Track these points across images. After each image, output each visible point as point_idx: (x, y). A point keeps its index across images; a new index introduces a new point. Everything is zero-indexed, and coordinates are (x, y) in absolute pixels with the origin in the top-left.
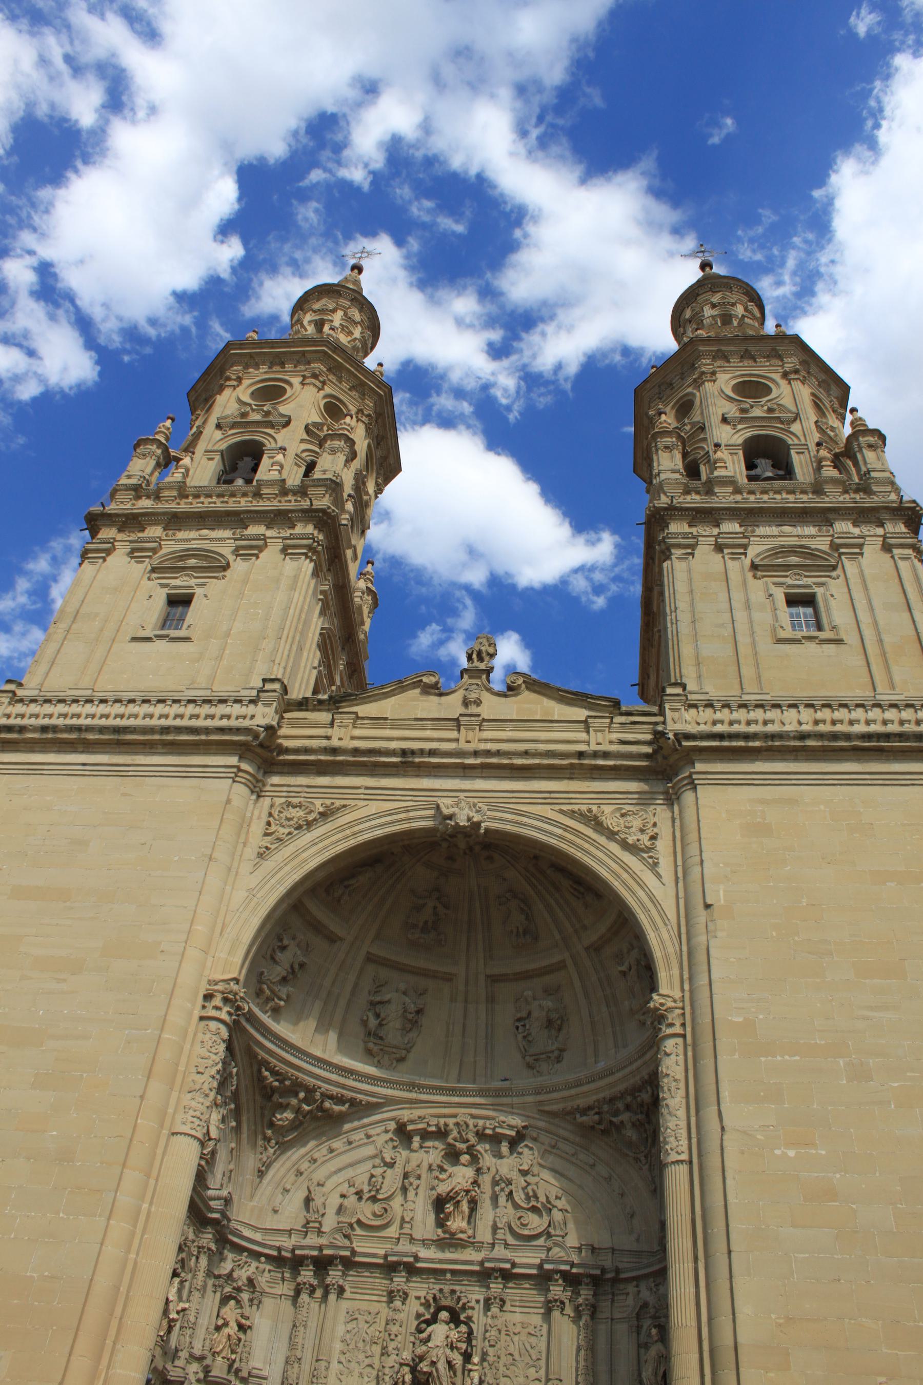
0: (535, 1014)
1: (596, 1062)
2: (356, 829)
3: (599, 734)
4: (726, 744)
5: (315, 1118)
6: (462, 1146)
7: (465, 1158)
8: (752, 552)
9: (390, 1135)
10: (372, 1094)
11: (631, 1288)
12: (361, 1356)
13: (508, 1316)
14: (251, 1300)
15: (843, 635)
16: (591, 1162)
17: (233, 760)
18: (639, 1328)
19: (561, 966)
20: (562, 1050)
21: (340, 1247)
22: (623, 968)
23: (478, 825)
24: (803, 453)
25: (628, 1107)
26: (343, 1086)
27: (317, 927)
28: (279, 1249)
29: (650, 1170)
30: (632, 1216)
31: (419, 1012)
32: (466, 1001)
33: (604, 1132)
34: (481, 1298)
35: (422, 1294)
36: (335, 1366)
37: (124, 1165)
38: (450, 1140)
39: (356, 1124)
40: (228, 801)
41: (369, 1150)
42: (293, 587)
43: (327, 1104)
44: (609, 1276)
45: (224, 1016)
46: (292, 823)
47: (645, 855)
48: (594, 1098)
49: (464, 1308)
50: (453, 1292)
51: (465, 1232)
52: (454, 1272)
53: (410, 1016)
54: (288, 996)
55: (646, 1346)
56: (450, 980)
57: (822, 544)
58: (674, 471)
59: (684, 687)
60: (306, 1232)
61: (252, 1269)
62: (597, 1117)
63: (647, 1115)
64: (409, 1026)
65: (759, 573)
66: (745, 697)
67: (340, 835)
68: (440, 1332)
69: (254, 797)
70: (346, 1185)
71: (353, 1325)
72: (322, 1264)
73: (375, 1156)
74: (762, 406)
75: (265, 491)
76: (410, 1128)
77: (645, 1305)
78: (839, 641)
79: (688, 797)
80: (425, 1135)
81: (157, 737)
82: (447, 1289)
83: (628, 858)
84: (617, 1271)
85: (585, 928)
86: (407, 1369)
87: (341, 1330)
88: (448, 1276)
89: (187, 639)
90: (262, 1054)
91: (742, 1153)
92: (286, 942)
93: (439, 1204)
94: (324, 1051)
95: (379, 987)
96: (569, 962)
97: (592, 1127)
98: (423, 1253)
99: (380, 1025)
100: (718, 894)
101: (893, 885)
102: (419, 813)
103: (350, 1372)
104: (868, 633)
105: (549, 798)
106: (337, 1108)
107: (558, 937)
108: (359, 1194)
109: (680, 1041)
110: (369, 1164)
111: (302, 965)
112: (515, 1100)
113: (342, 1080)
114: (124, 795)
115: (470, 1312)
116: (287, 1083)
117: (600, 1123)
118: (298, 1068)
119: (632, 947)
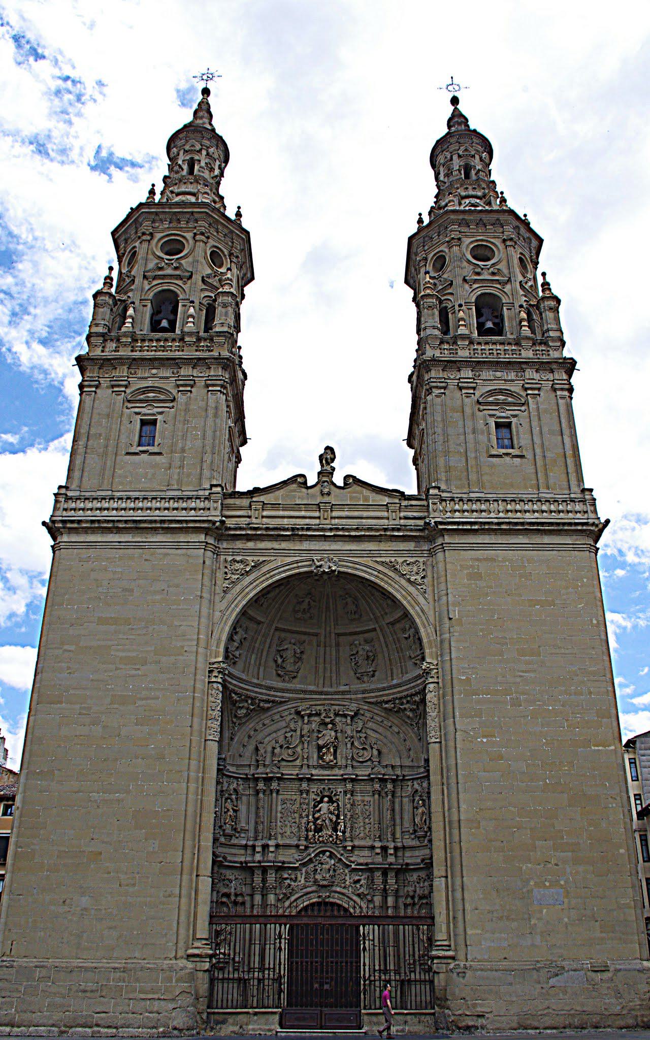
0: (361, 653)
1: (392, 680)
2: (272, 574)
3: (394, 514)
4: (460, 527)
5: (257, 711)
6: (328, 720)
7: (330, 726)
8: (478, 393)
9: (292, 716)
10: (283, 697)
11: (410, 783)
12: (290, 819)
13: (355, 798)
14: (237, 799)
15: (525, 453)
16: (390, 725)
17: (202, 537)
18: (414, 800)
19: (374, 630)
20: (374, 671)
21: (276, 772)
22: (406, 636)
23: (335, 571)
24: (510, 309)
25: (408, 702)
26: (269, 695)
27: (251, 619)
28: (246, 775)
29: (418, 730)
30: (410, 750)
31: (302, 652)
32: (325, 646)
33: (396, 712)
34: (342, 790)
35: (315, 790)
36: (279, 824)
37: (189, 759)
38: (322, 717)
39: (276, 711)
40: (204, 562)
41: (283, 724)
42: (216, 415)
43: (261, 704)
44: (401, 778)
45: (220, 680)
46: (238, 572)
47: (419, 587)
48: (392, 697)
49: (335, 795)
50: (329, 789)
51: (332, 761)
52: (329, 780)
53: (297, 655)
54: (240, 655)
55: (417, 808)
56: (317, 636)
57: (516, 388)
58: (434, 327)
59: (439, 488)
60: (258, 766)
61: (235, 785)
62: (393, 706)
63: (418, 706)
64: (297, 660)
65: (482, 408)
66: (472, 495)
67: (264, 578)
68: (324, 806)
69: (215, 556)
70: (274, 742)
71: (285, 805)
72: (268, 780)
73: (286, 727)
74: (488, 269)
75: (187, 339)
76: (303, 713)
77: (417, 791)
78: (522, 457)
79: (440, 555)
80: (310, 715)
81: (158, 525)
82: (327, 788)
83: (411, 589)
84: (404, 776)
85: (386, 614)
86: (312, 824)
87: (279, 808)
88: (326, 781)
89: (160, 454)
90: (231, 687)
91: (464, 740)
92: (237, 630)
93: (320, 748)
94: (258, 679)
95: (281, 641)
96: (378, 629)
97: (390, 710)
98: (314, 772)
99: (283, 661)
100: (455, 614)
101: (538, 607)
102: (303, 564)
103: (286, 826)
104: (538, 451)
105: (370, 554)
106: (266, 705)
107: (372, 617)
108: (281, 747)
109: (435, 685)
110: (284, 730)
111: (245, 638)
112: (353, 696)
113: (268, 692)
114: (146, 560)
115: (338, 797)
116: (243, 697)
117: (394, 708)
118: (247, 690)
119: (410, 627)
